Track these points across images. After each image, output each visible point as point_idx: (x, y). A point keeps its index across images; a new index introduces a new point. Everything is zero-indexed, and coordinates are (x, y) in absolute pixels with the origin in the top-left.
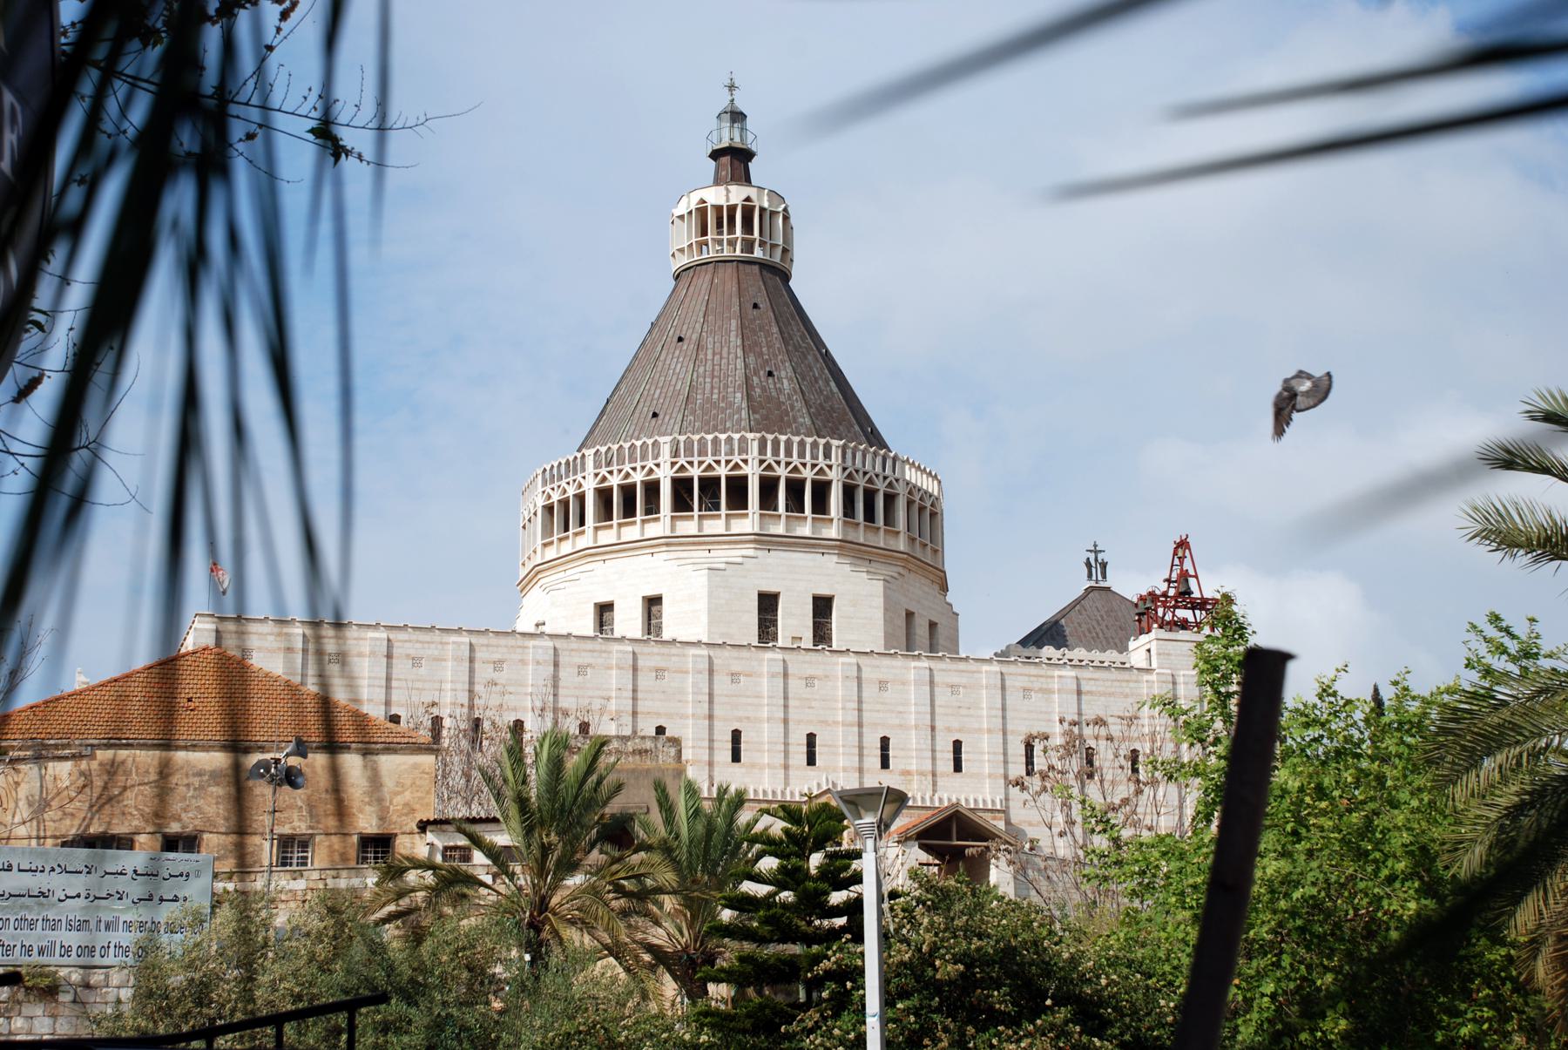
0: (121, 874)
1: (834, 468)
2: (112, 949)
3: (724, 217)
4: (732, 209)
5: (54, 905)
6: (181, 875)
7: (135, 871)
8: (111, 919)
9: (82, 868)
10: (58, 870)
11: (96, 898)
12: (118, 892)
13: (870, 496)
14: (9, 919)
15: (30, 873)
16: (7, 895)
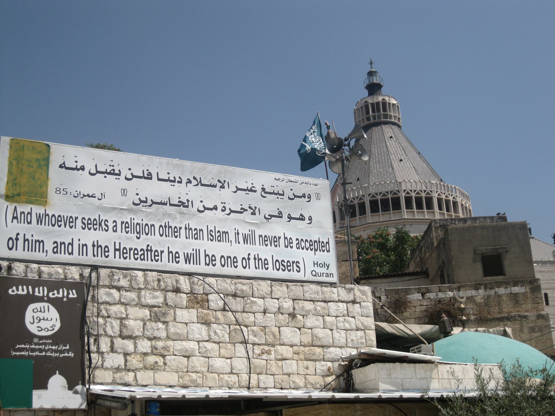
0: (251, 190)
1: (433, 192)
2: (252, 261)
3: (376, 106)
4: (378, 103)
5: (194, 215)
6: (304, 196)
7: (263, 189)
8: (247, 232)
9: (215, 182)
10: (194, 182)
11: (232, 211)
12: (250, 208)
13: (447, 202)
14: (153, 225)
15: (169, 183)
16: (149, 203)
